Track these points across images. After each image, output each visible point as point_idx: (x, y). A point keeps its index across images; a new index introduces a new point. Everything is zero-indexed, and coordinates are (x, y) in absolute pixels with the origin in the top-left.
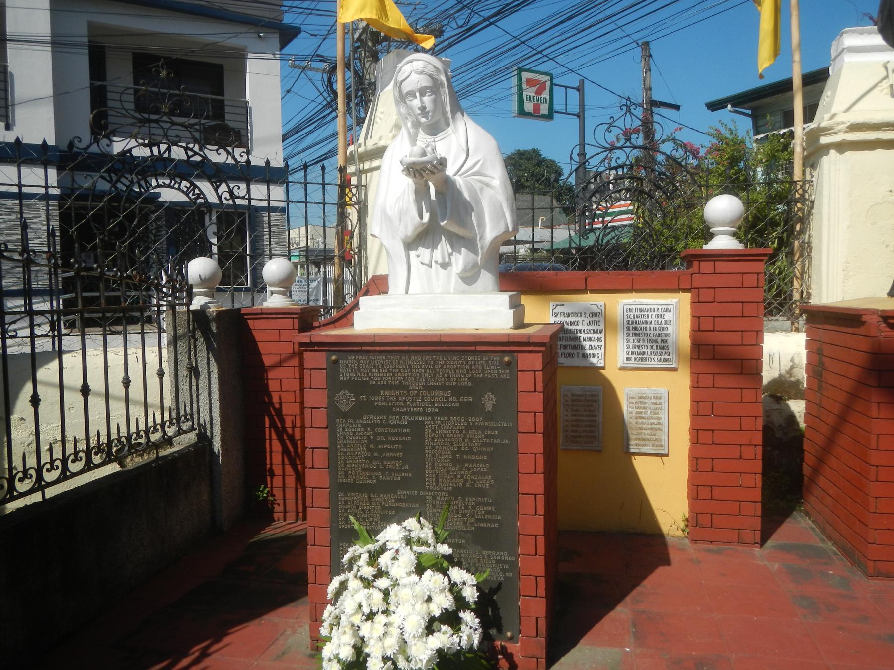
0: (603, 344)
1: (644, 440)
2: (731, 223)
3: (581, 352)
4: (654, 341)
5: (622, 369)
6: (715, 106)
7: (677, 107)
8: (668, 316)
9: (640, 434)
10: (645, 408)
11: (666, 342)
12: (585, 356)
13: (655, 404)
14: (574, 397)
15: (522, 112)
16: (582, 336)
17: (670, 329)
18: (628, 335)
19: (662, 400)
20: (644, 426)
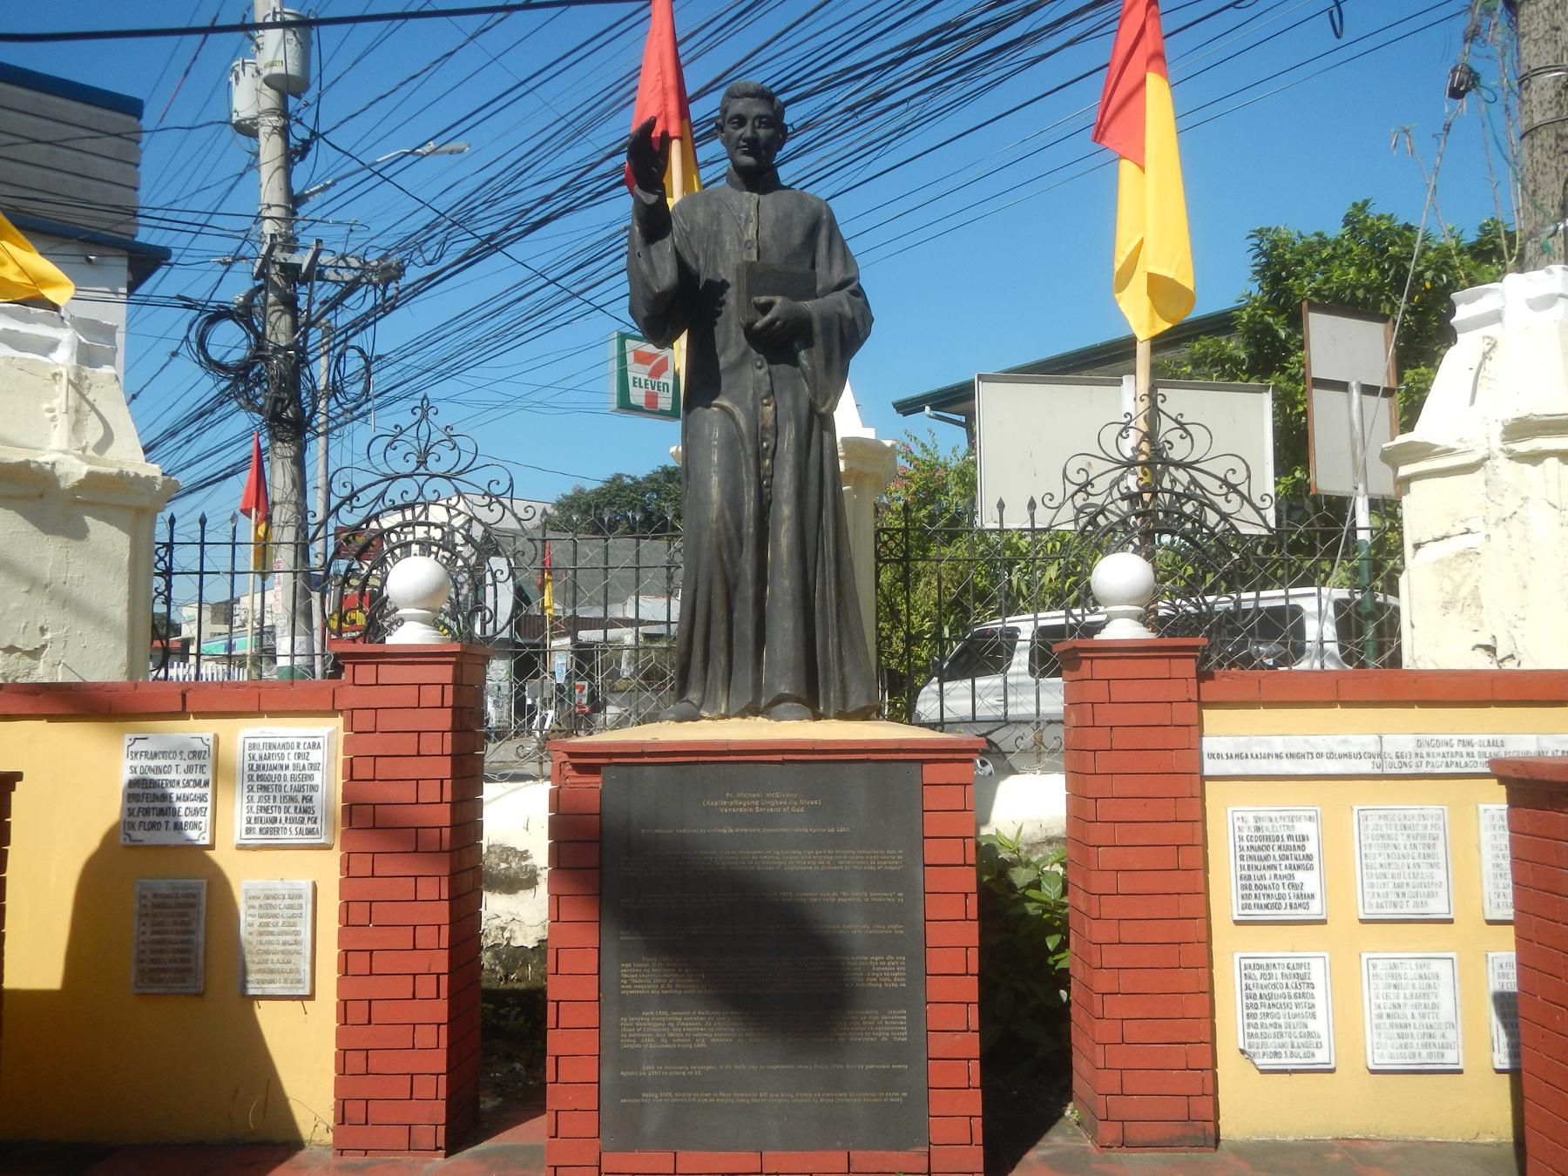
0: (208, 805)
1: (271, 971)
2: (417, 602)
3: (172, 820)
4: (292, 799)
5: (241, 847)
6: (907, 407)
8: (316, 756)
9: (266, 962)
10: (275, 916)
11: (311, 800)
12: (178, 827)
13: (291, 907)
14: (159, 900)
15: (625, 405)
16: (175, 792)
17: (318, 779)
18: (251, 789)
19: (302, 901)
20: (271, 948)
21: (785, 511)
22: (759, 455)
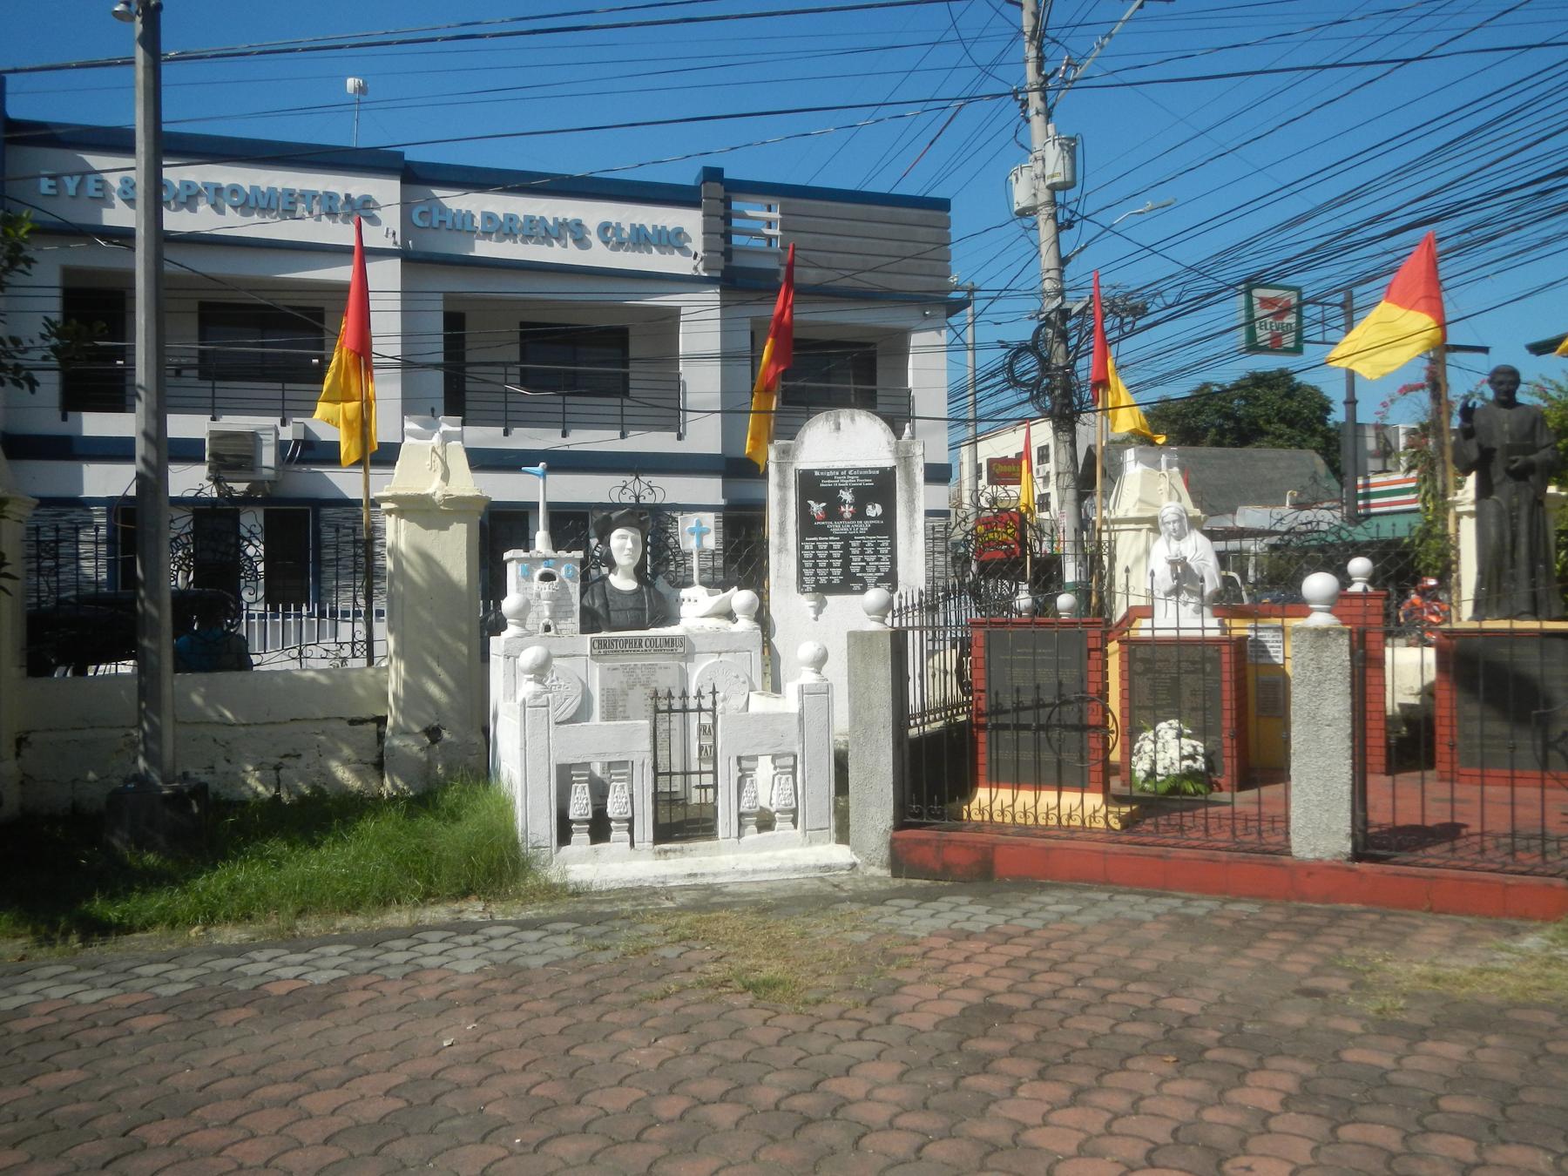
7: (1485, 350)
21: (1523, 540)
22: (1512, 518)
